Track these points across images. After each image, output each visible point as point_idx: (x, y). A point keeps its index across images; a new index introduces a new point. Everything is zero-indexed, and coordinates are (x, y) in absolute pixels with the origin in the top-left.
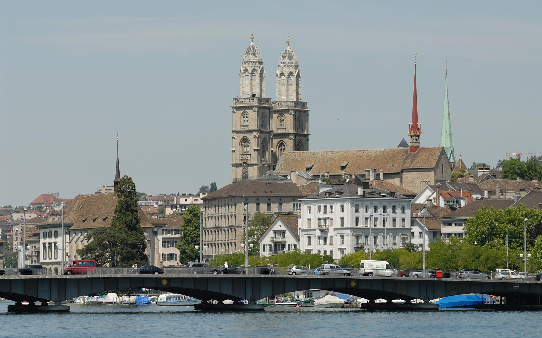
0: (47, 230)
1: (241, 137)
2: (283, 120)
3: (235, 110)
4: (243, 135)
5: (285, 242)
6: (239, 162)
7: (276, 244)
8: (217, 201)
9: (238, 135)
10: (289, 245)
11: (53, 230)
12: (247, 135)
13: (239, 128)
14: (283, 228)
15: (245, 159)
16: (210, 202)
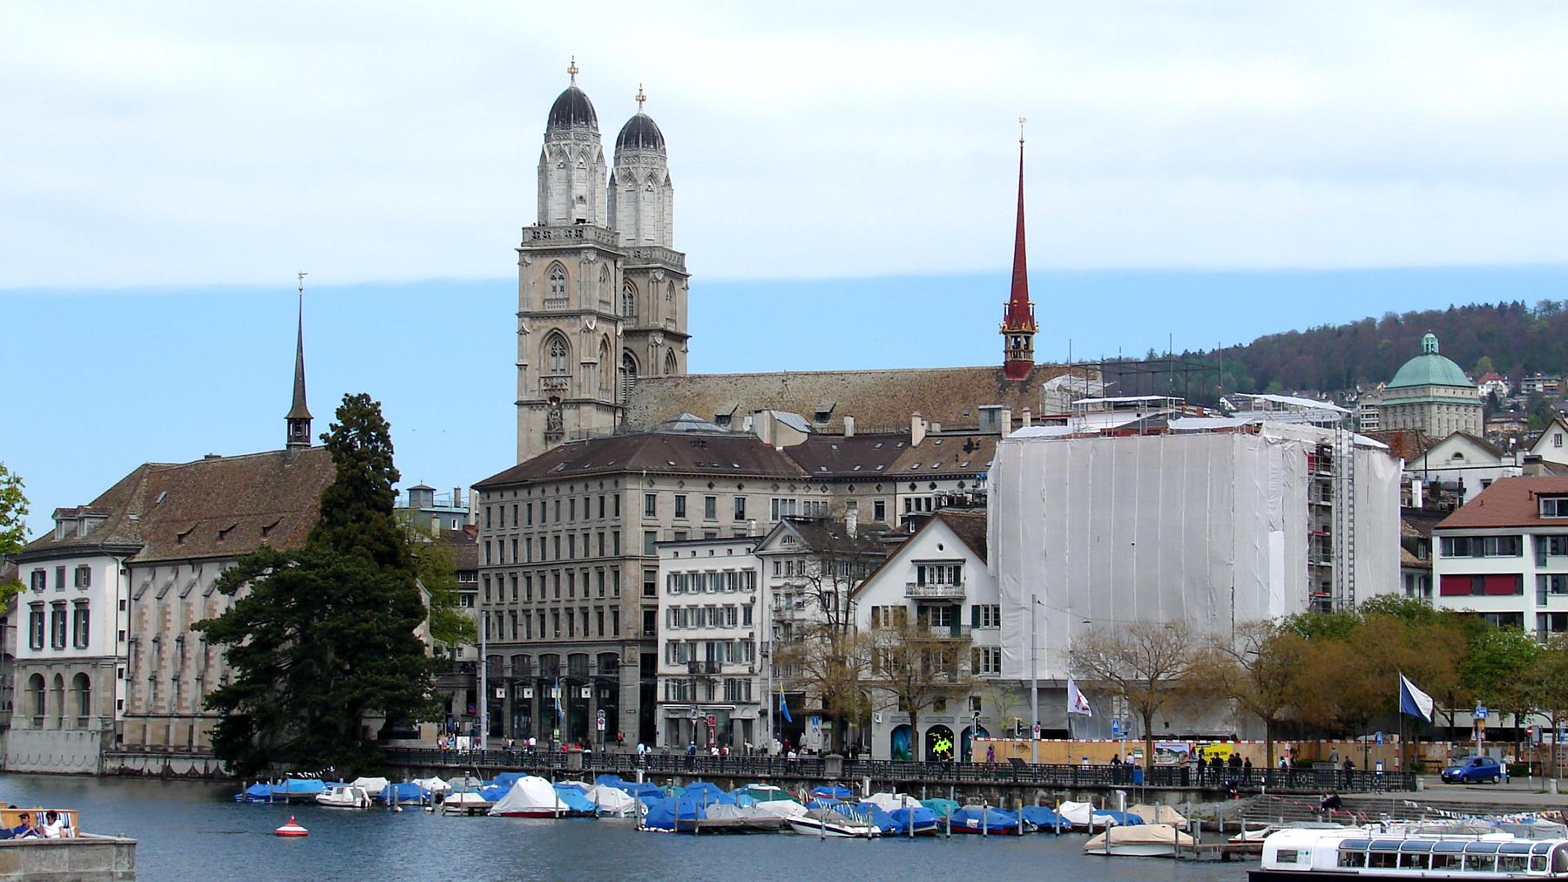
0: (50, 569)
1: (544, 331)
2: (631, 296)
3: (528, 259)
4: (551, 324)
5: (962, 599)
6: (534, 397)
7: (923, 605)
8: (536, 492)
9: (537, 324)
10: (976, 609)
11: (71, 567)
12: (562, 325)
13: (536, 307)
14: (954, 550)
15: (554, 388)
16: (508, 495)
